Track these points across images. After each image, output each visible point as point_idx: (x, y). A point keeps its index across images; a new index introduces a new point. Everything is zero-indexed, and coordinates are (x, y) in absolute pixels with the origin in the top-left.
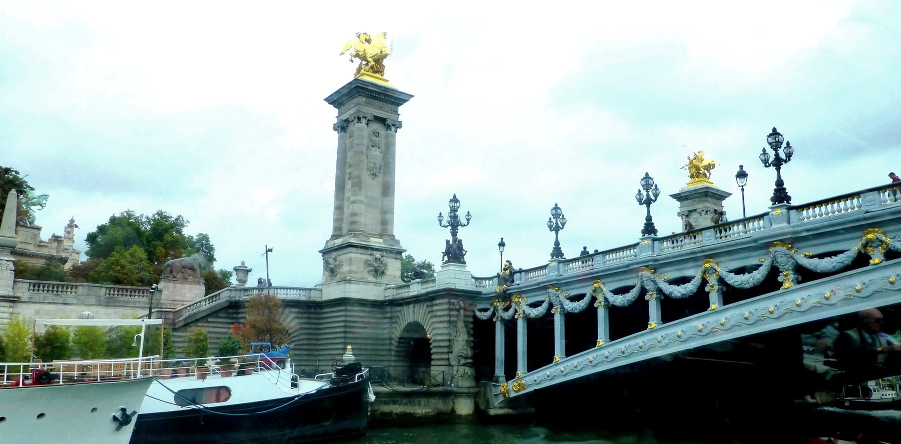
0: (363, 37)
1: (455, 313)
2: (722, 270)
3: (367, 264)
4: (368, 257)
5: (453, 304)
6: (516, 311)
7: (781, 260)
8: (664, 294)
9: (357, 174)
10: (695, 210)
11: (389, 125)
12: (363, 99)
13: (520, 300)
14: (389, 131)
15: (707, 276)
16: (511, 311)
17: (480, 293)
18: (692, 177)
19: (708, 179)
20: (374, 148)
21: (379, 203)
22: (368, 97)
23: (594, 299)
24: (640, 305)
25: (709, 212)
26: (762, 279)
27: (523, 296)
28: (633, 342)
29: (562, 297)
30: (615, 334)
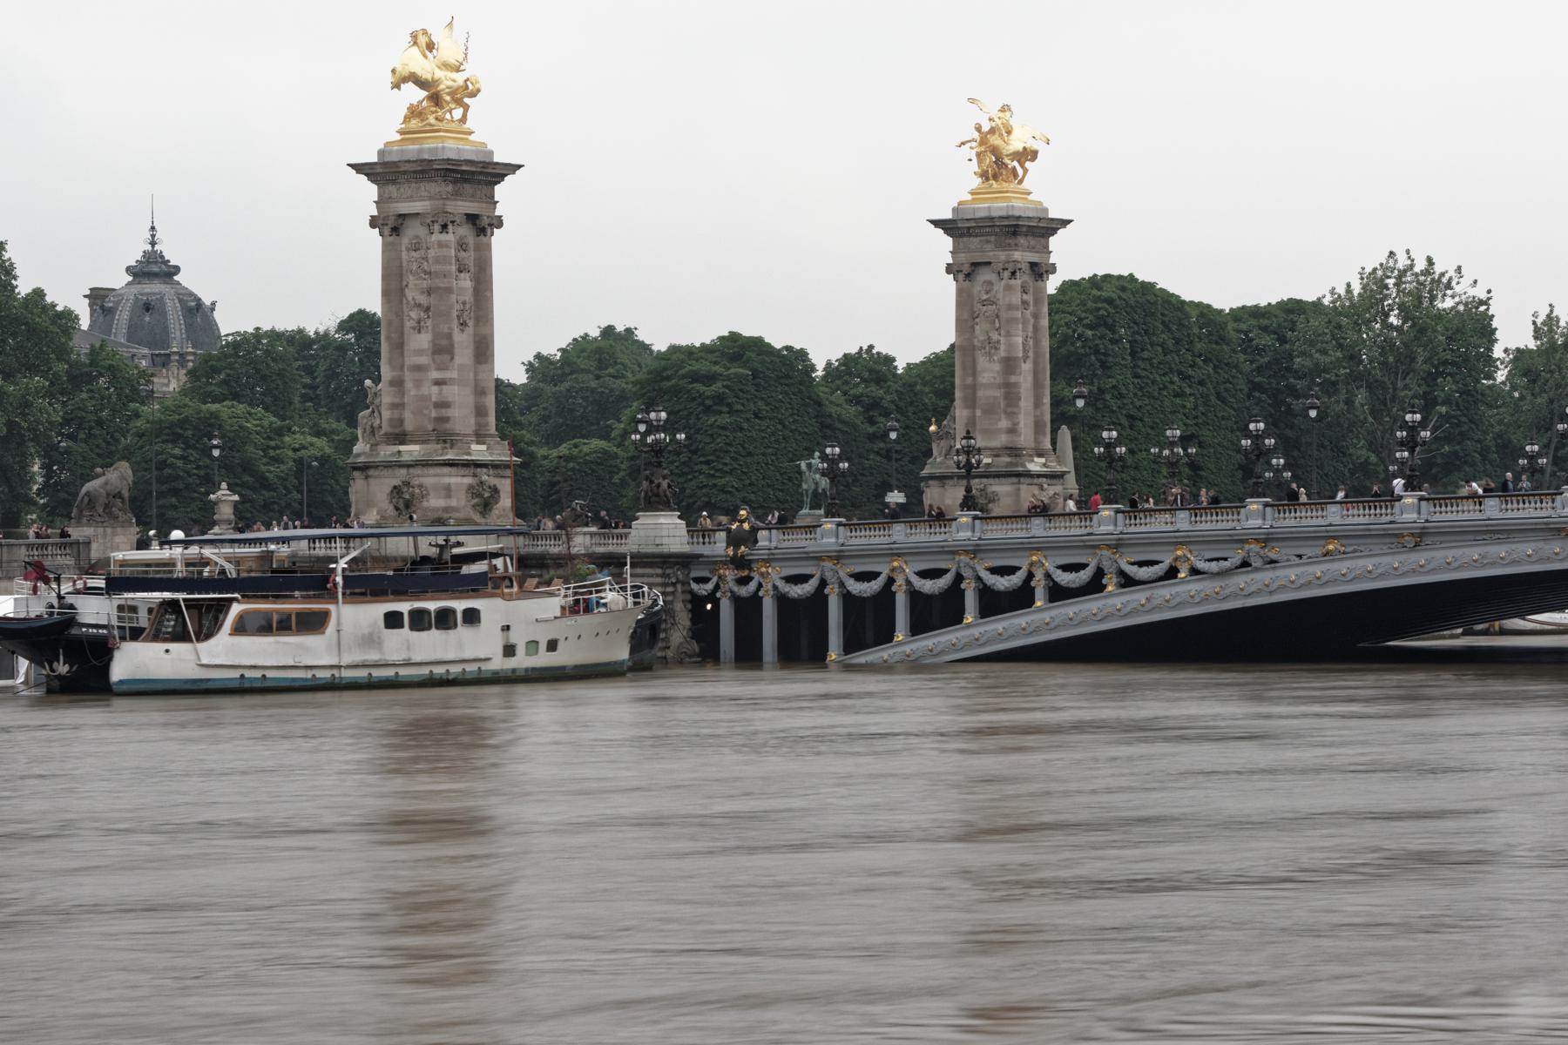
0: (422, 40)
1: (670, 589)
2: (1049, 565)
3: (473, 492)
4: (468, 480)
5: (668, 576)
6: (760, 586)
7: (1106, 565)
8: (985, 585)
9: (446, 330)
10: (989, 263)
11: (483, 225)
12: (450, 188)
13: (770, 570)
14: (482, 237)
15: (1033, 570)
16: (752, 586)
17: (702, 556)
18: (984, 175)
19: (1021, 182)
20: (462, 274)
21: (472, 375)
22: (455, 181)
23: (891, 581)
24: (955, 592)
25: (1018, 274)
26: (1088, 580)
27: (773, 564)
28: (943, 639)
29: (841, 573)
30: (918, 627)
